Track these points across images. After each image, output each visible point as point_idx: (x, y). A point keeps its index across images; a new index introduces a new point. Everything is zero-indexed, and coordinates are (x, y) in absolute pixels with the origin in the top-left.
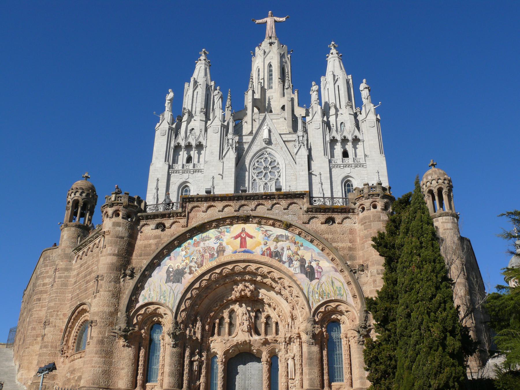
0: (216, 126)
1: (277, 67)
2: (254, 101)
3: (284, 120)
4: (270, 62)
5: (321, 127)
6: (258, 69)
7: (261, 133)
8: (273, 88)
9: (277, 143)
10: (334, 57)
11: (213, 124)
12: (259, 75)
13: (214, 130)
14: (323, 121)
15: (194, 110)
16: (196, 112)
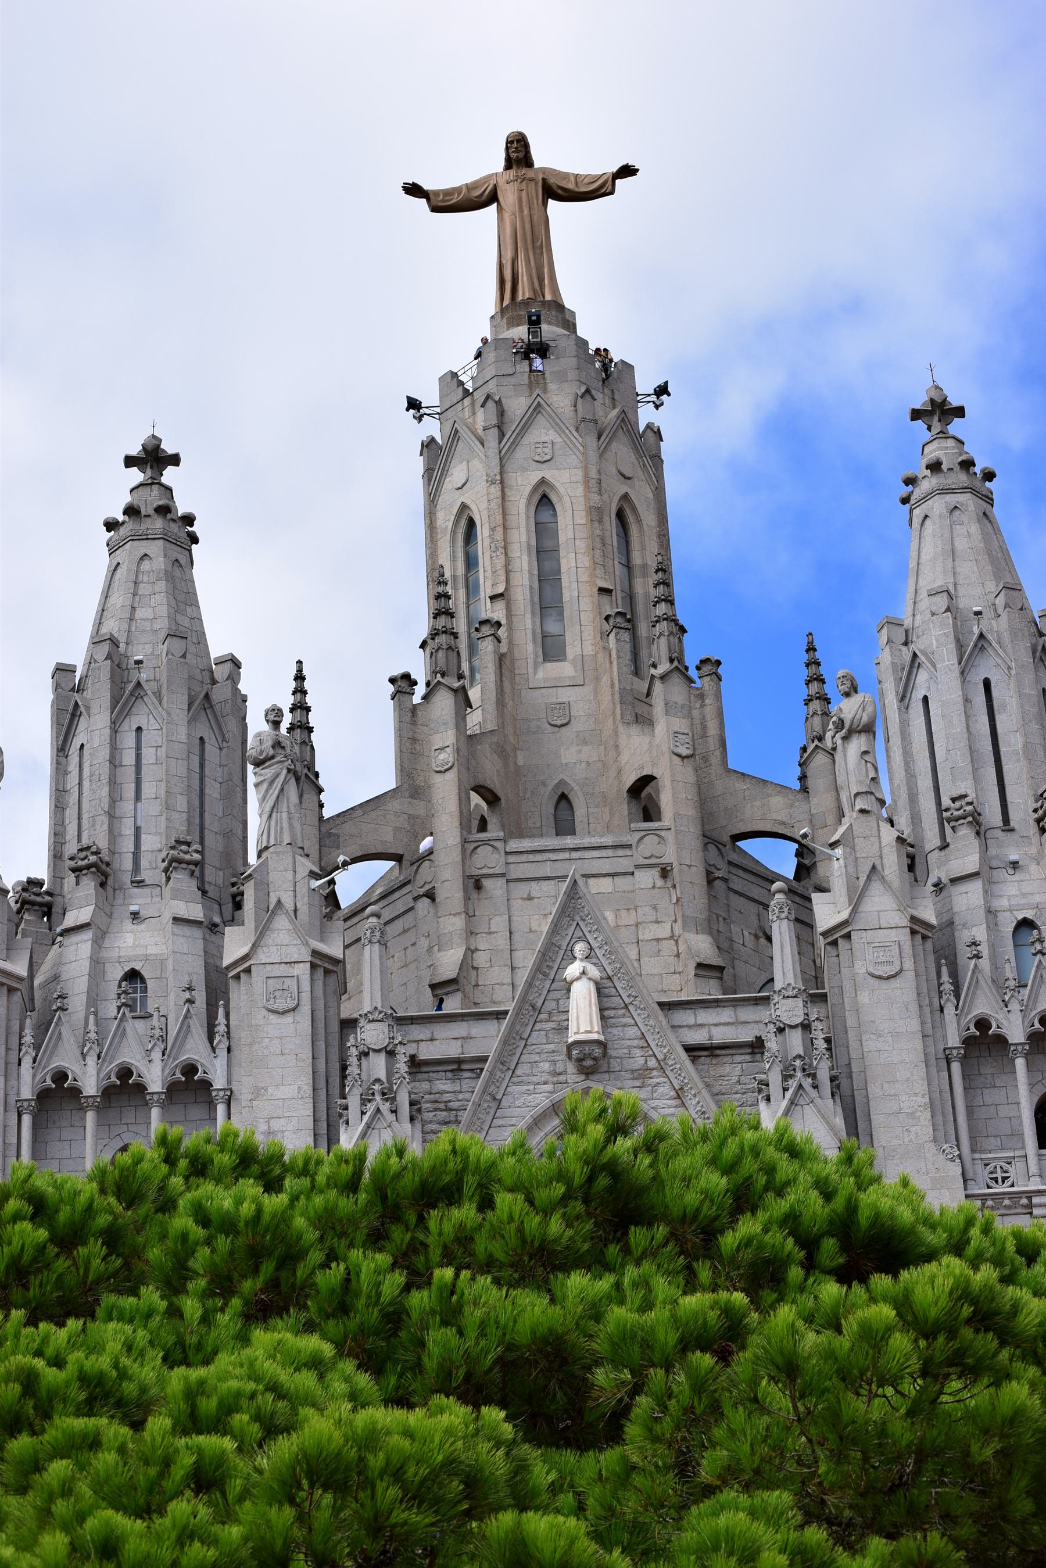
0: (283, 970)
1: (581, 518)
2: (469, 742)
3: (660, 882)
4: (543, 482)
5: (909, 965)
6: (463, 523)
7: (551, 1005)
8: (572, 651)
9: (652, 1063)
10: (950, 491)
11: (262, 956)
12: (471, 562)
13: (271, 996)
14: (918, 928)
15: (127, 845)
16: (144, 863)
